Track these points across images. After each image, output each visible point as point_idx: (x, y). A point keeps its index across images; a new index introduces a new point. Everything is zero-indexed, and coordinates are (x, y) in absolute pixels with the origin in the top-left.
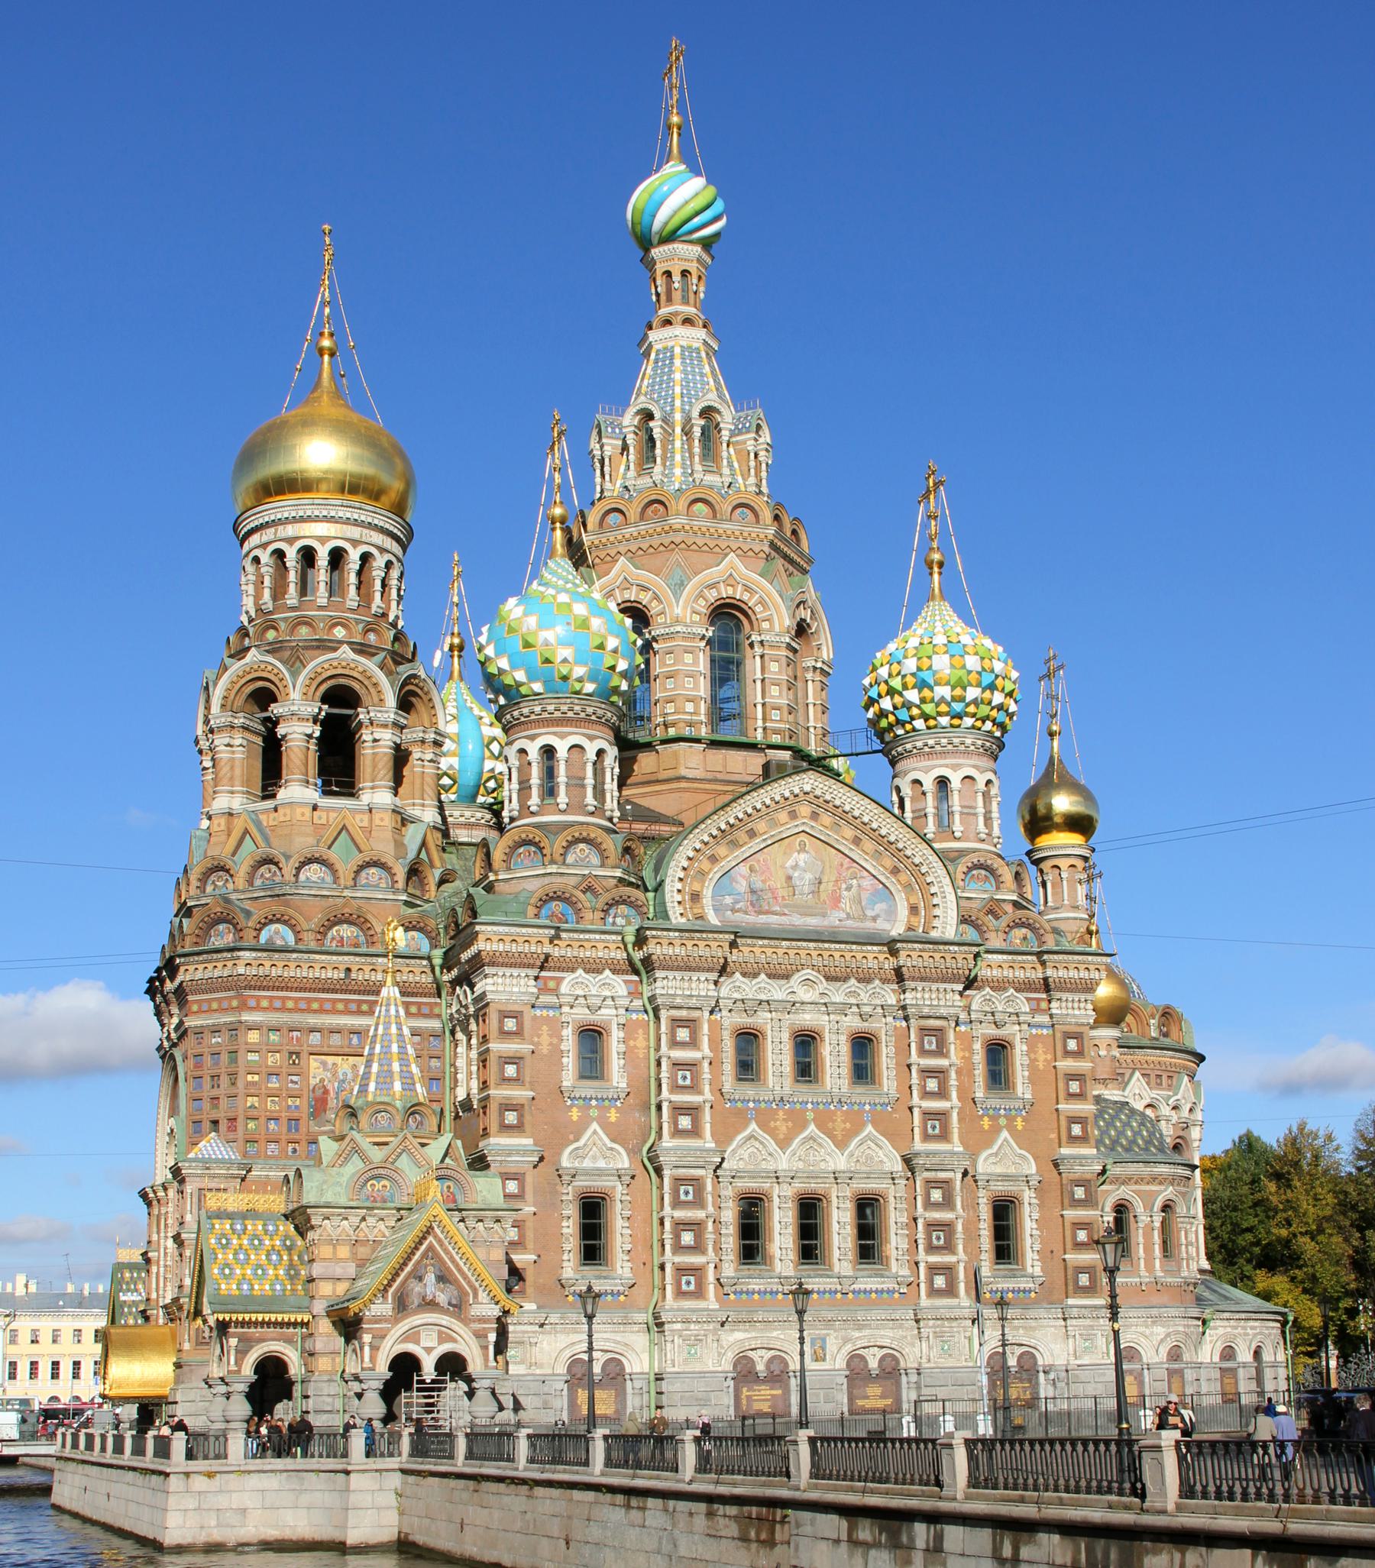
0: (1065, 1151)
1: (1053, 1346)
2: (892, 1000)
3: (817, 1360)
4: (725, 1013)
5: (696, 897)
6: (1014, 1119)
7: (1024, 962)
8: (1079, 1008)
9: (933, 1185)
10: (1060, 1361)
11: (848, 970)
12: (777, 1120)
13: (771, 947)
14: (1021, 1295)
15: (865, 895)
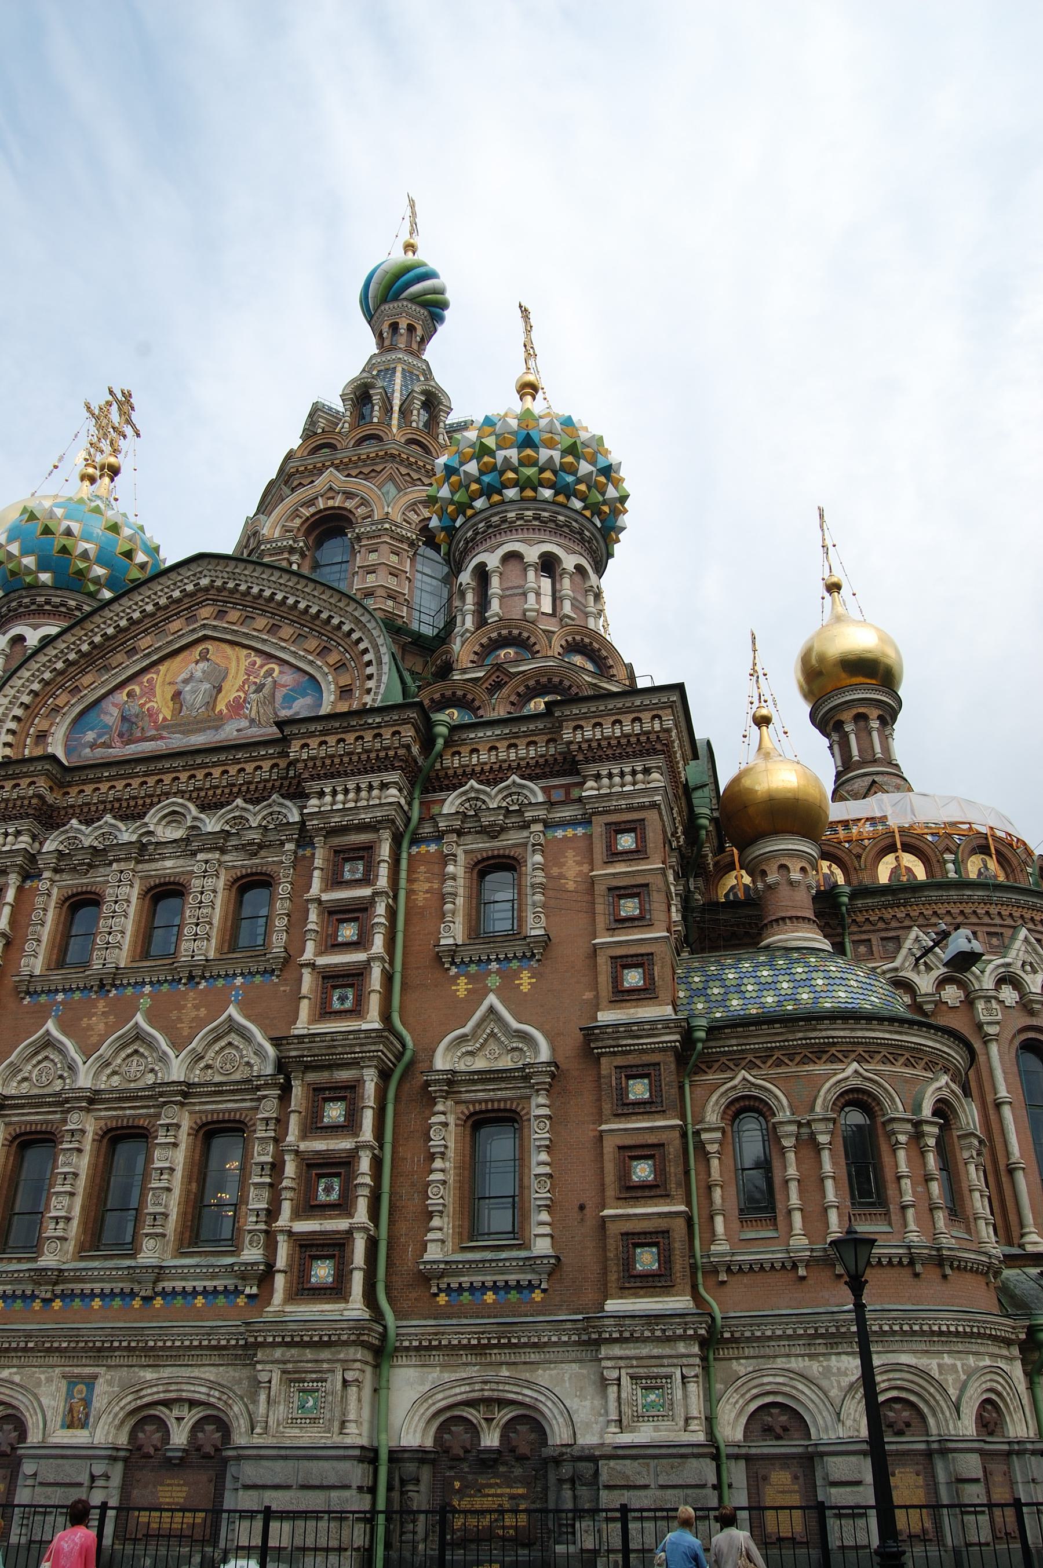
0: (606, 1017)
1: (573, 1403)
2: (294, 817)
3: (70, 1426)
4: (47, 874)
5: (42, 737)
6: (516, 974)
7: (533, 732)
8: (634, 784)
9: (327, 1094)
10: (588, 1439)
11: (235, 790)
12: (95, 1014)
13: (122, 777)
14: (513, 1296)
15: (279, 695)
